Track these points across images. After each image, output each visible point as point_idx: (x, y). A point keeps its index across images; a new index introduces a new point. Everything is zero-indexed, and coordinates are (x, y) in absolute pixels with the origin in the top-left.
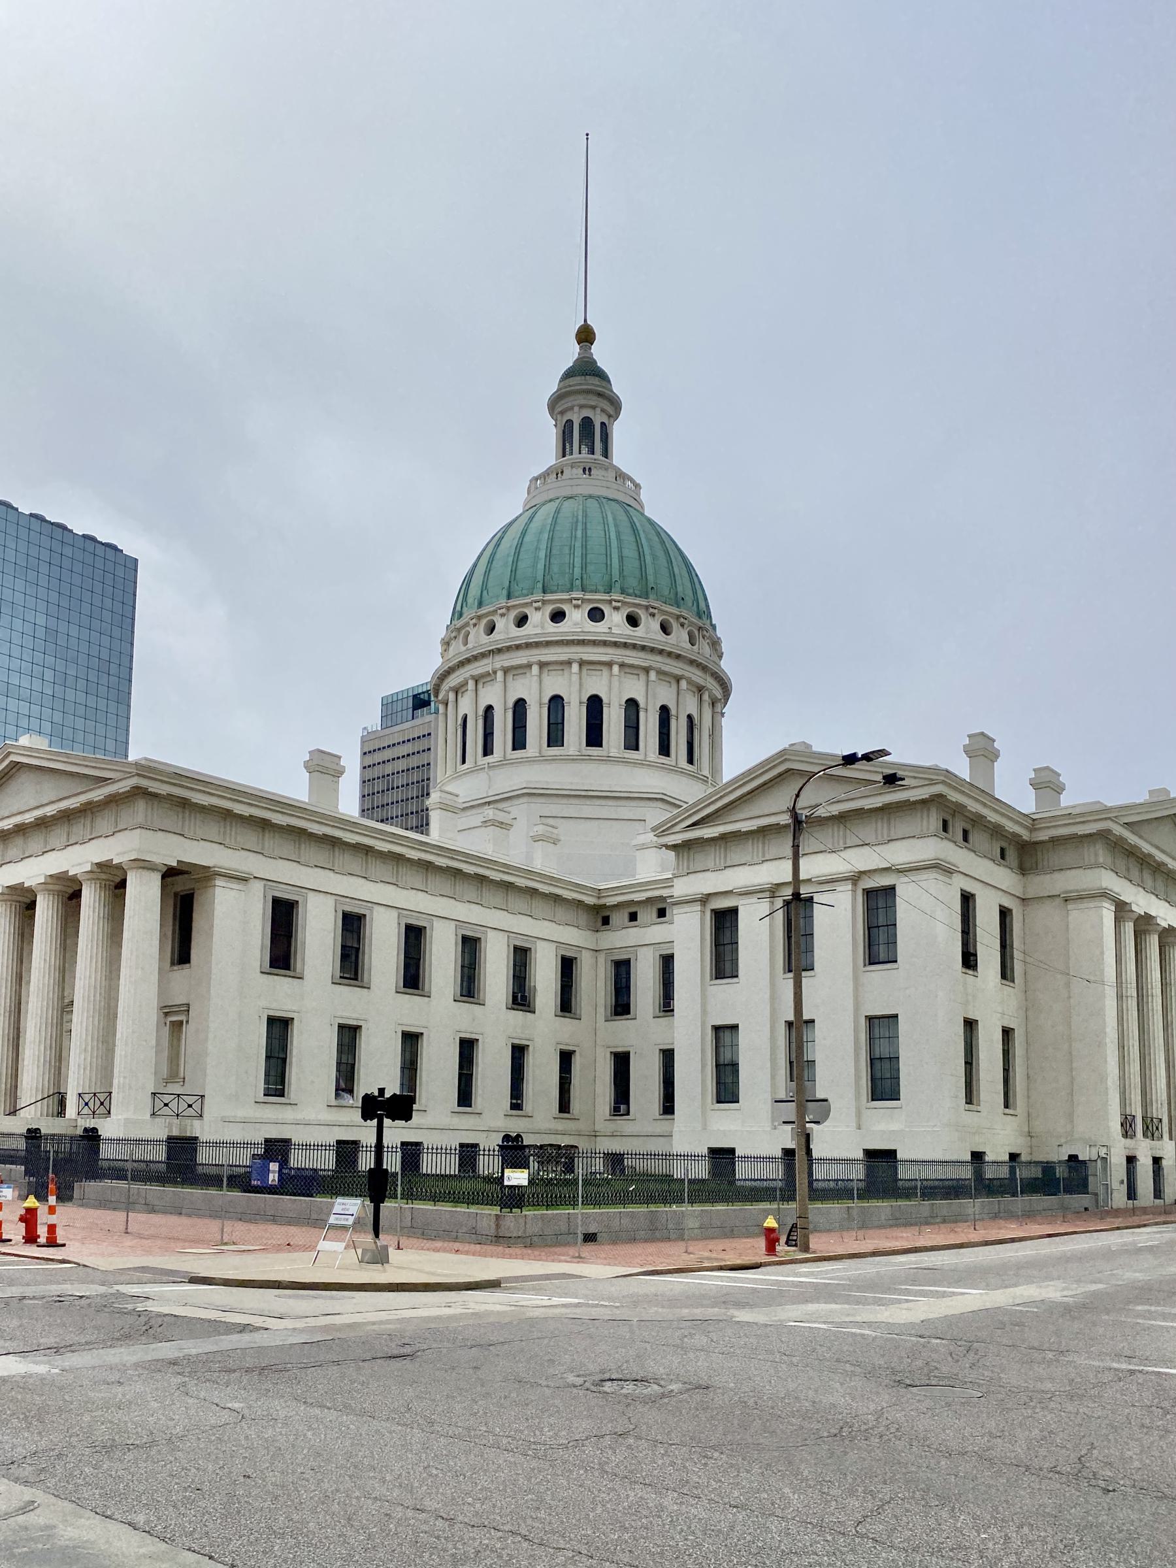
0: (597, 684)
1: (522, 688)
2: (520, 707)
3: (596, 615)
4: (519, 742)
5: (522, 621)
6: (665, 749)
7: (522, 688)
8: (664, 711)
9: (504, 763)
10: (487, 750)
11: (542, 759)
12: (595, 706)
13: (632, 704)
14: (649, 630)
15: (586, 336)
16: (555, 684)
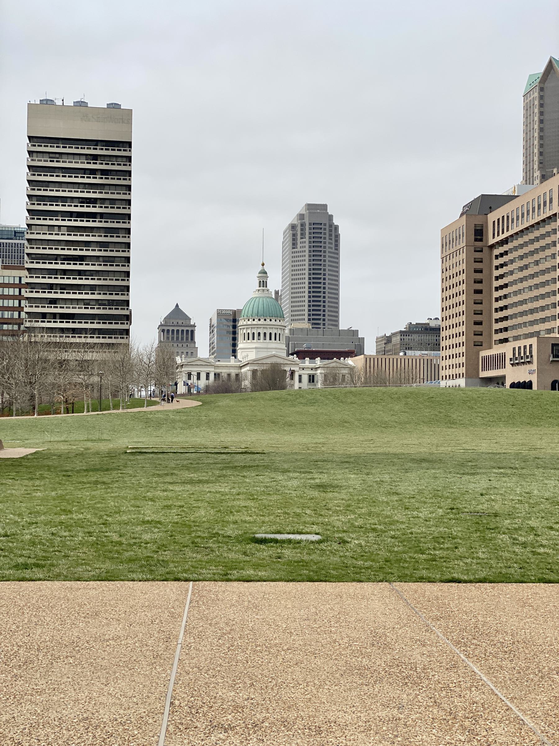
0: (265, 331)
1: (254, 331)
2: (254, 333)
3: (265, 320)
4: (253, 339)
5: (254, 320)
6: (275, 340)
7: (254, 331)
8: (275, 334)
9: (251, 342)
10: (248, 339)
11: (257, 342)
12: (265, 334)
13: (270, 334)
14: (273, 322)
15: (263, 265)
16: (259, 331)
